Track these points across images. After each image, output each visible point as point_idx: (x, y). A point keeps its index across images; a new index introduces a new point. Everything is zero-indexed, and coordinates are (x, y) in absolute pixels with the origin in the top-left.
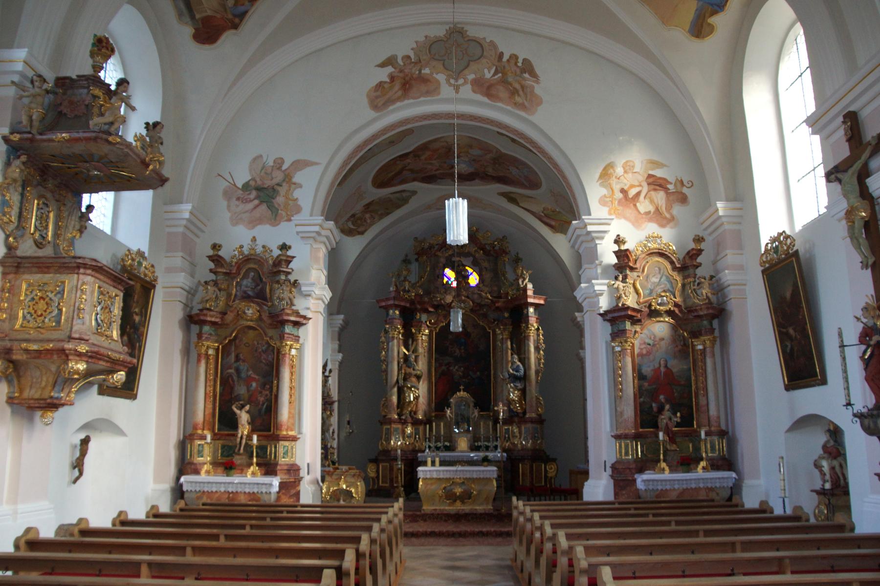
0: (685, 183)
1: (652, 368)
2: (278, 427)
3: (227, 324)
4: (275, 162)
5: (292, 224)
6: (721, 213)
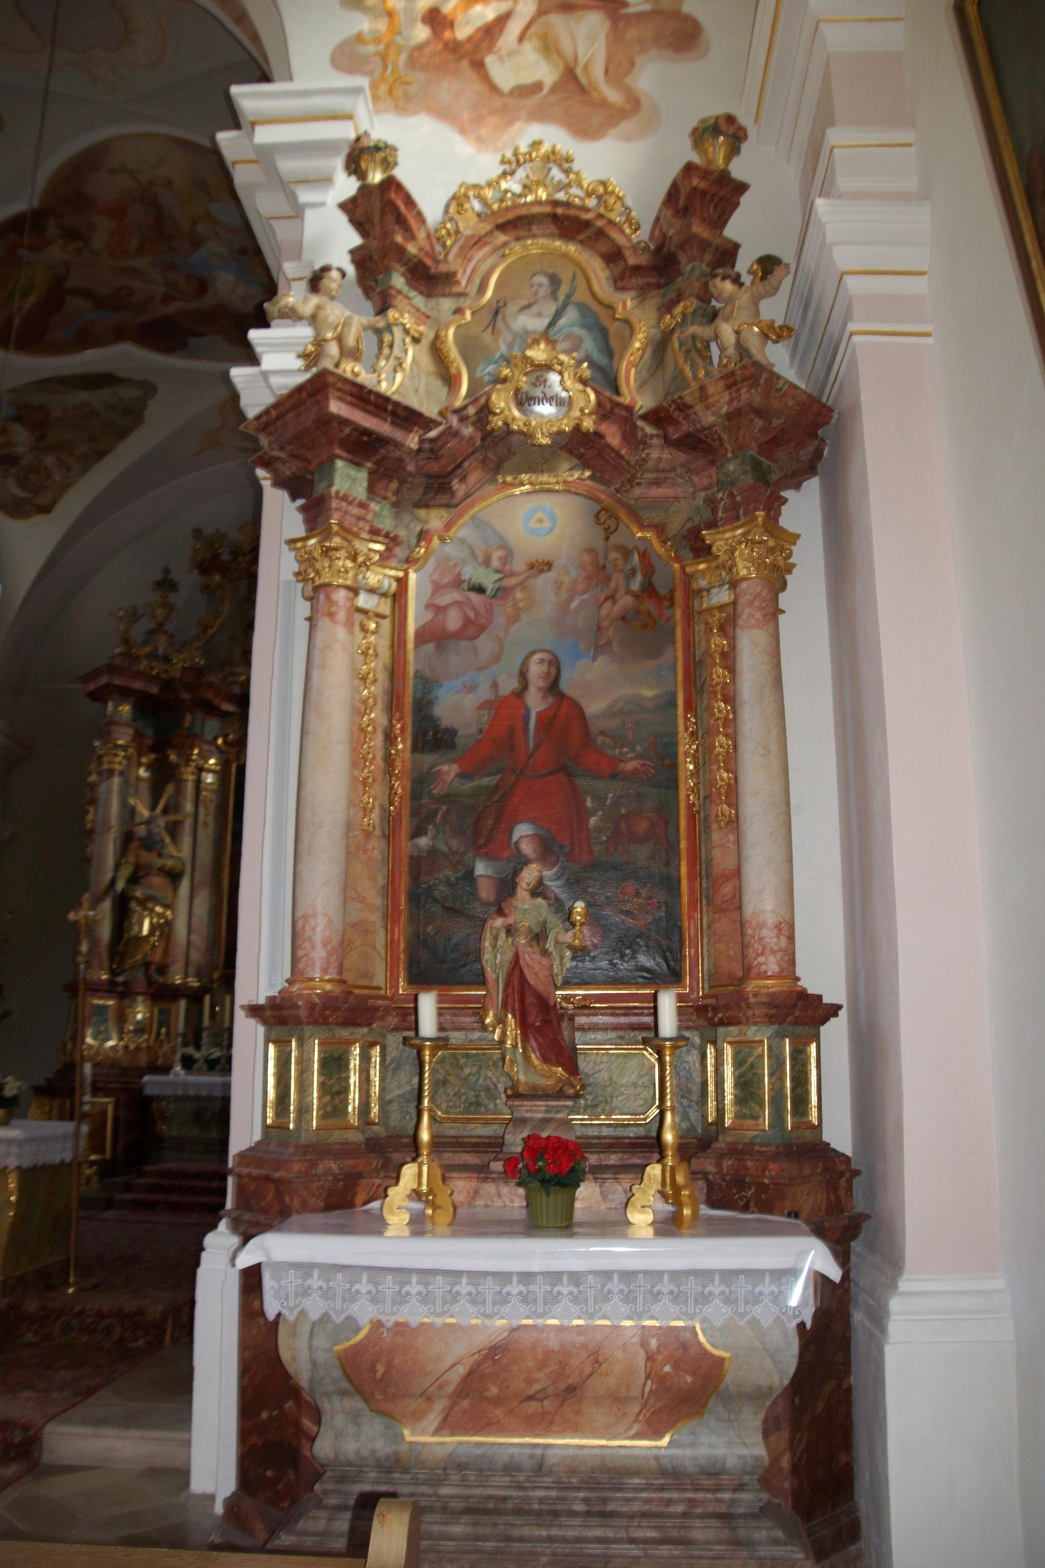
1: (484, 693)
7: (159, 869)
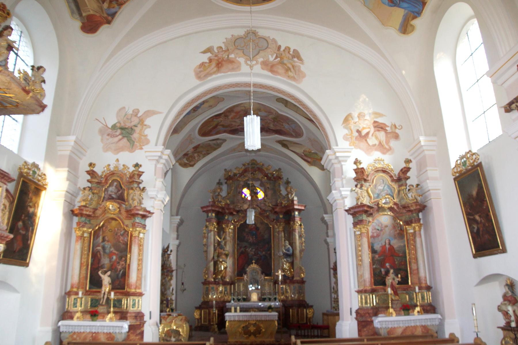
0: (397, 126)
1: (380, 245)
2: (129, 286)
3: (98, 217)
4: (133, 111)
5: (143, 151)
6: (422, 143)
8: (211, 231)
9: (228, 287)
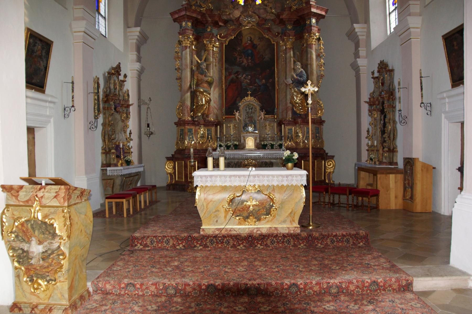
7: (206, 81)
8: (186, 47)
9: (213, 129)
